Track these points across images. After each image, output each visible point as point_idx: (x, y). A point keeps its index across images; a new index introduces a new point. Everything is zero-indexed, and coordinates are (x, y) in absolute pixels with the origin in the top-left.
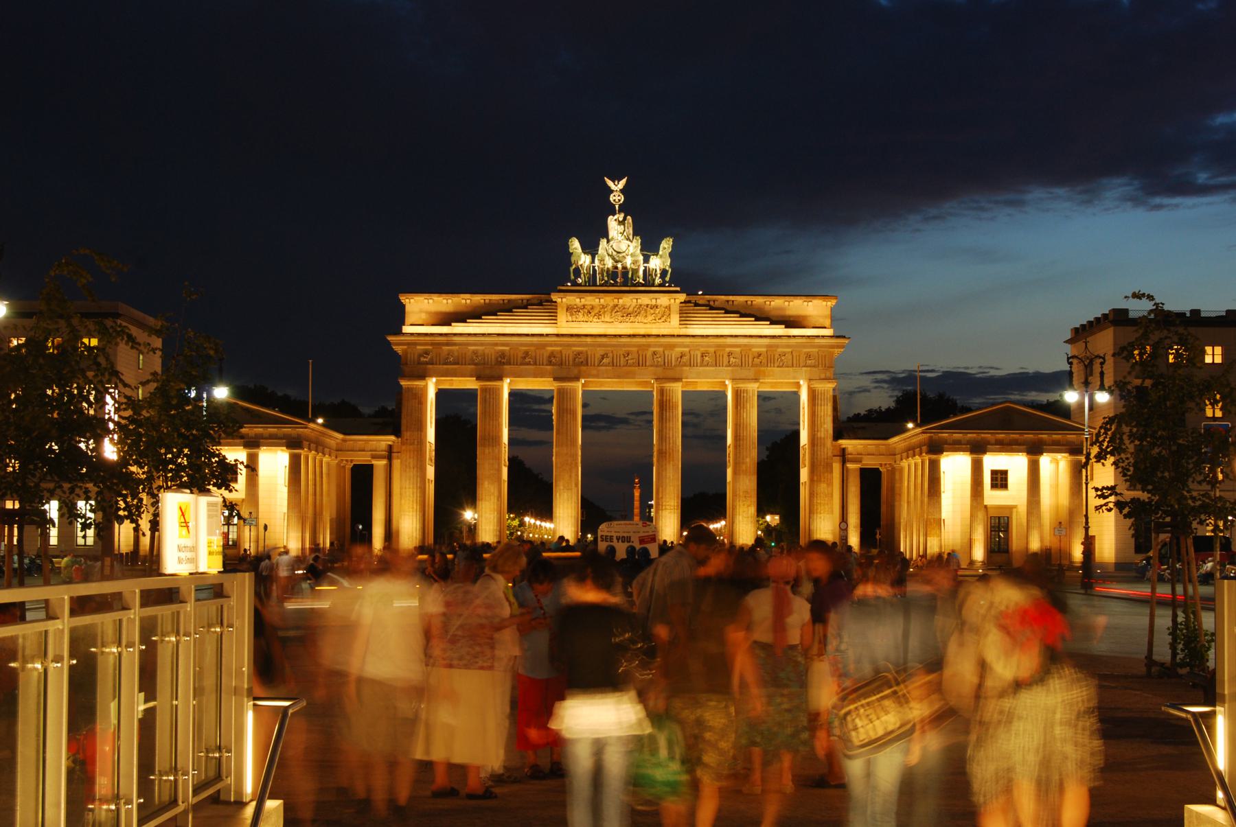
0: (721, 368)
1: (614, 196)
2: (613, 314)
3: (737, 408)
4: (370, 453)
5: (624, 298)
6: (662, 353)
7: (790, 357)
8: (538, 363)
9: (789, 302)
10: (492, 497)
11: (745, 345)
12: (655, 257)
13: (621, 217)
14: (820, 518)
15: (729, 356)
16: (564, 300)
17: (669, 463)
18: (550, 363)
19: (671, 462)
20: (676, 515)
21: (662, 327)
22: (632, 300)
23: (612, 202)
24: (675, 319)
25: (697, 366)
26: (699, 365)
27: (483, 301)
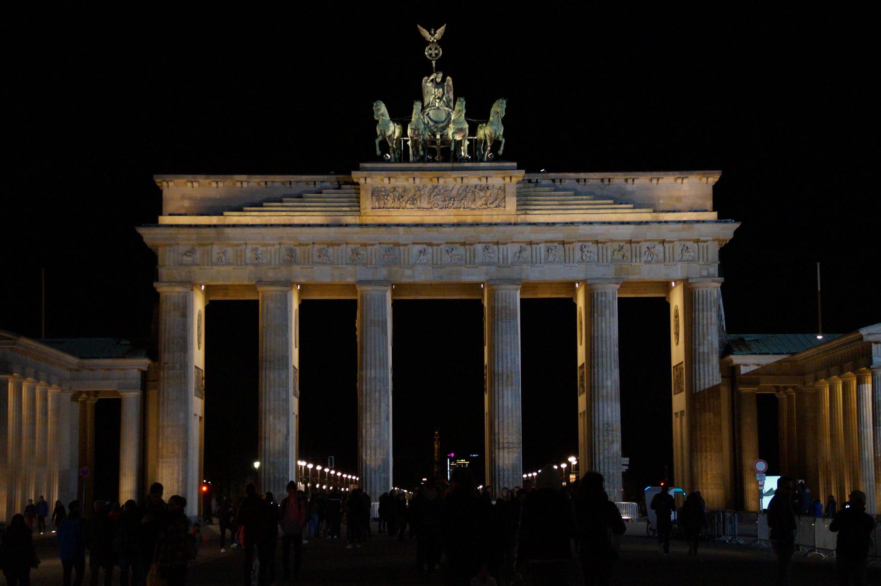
0: (571, 264)
1: (430, 49)
4: (117, 381)
5: (444, 176)
7: (662, 248)
9: (658, 179)
11: (603, 234)
12: (484, 125)
13: (441, 75)
14: (706, 458)
16: (369, 180)
17: (507, 389)
18: (353, 262)
19: (510, 388)
21: (495, 213)
24: (511, 204)
25: (540, 263)
26: (543, 261)
27: (264, 184)
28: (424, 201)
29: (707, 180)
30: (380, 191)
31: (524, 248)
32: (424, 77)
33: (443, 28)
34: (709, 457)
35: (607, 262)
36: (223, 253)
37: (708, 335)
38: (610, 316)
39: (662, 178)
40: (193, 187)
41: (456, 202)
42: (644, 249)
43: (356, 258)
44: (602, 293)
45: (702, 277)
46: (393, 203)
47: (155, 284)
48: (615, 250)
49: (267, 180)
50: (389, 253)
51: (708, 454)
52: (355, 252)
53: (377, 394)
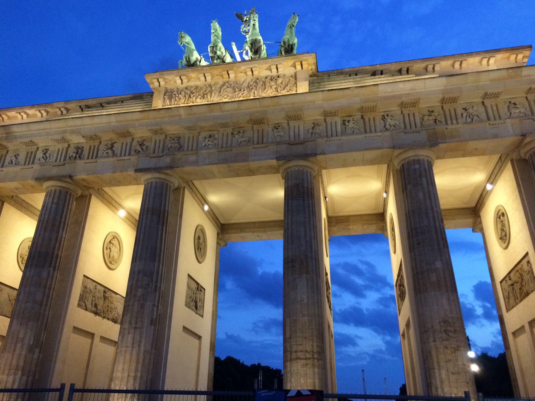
0: (372, 135)
1: (244, 27)
2: (222, 91)
3: (406, 189)
5: (234, 68)
6: (287, 124)
7: (482, 109)
8: (118, 155)
10: (19, 345)
15: (385, 118)
16: (162, 83)
18: (137, 152)
20: (316, 370)
22: (246, 73)
24: (303, 87)
25: (337, 136)
26: (339, 134)
27: (78, 108)
28: (215, 95)
29: (516, 58)
30: (172, 92)
35: (416, 127)
36: (15, 155)
38: (428, 185)
39: (466, 60)
40: (23, 119)
41: (246, 91)
43: (140, 149)
44: (414, 160)
46: (183, 99)
48: (423, 117)
49: (80, 105)
50: (174, 141)
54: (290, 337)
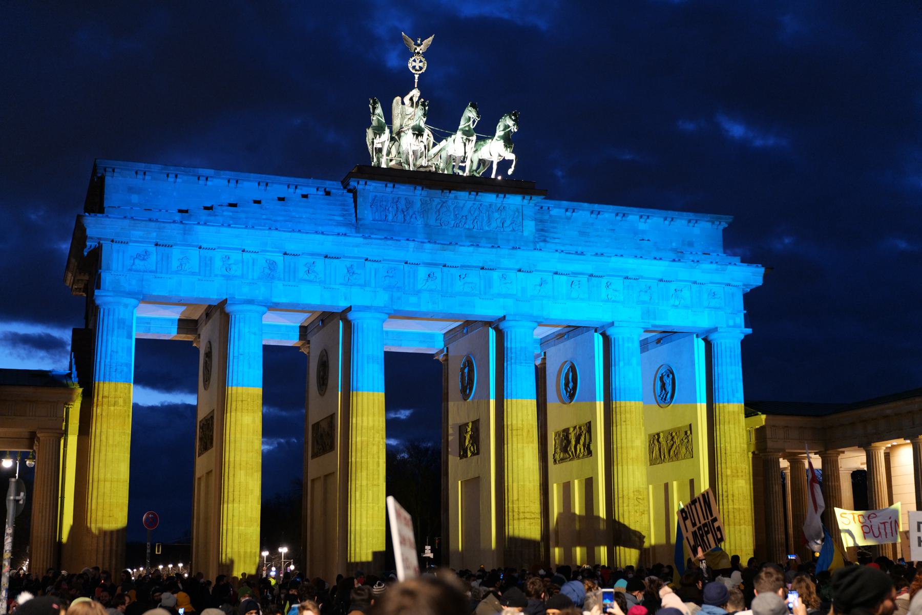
1: (414, 61)
9: (672, 219)
12: (490, 140)
14: (740, 531)
23: (411, 69)
24: (529, 227)
31: (545, 280)
32: (396, 97)
33: (431, 39)
34: (743, 530)
37: (737, 392)
42: (672, 291)
45: (728, 326)
47: (97, 292)
51: (743, 527)
52: (350, 271)
53: (375, 448)
54: (518, 500)
